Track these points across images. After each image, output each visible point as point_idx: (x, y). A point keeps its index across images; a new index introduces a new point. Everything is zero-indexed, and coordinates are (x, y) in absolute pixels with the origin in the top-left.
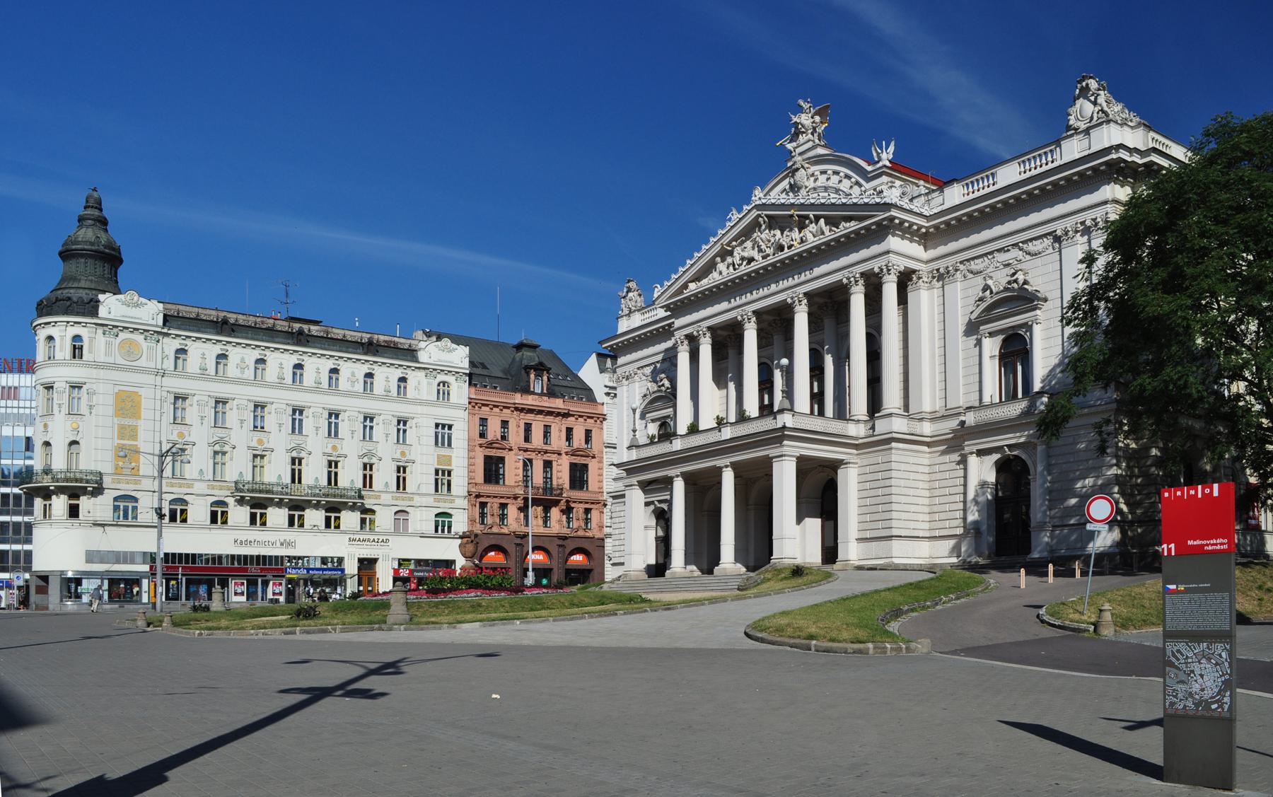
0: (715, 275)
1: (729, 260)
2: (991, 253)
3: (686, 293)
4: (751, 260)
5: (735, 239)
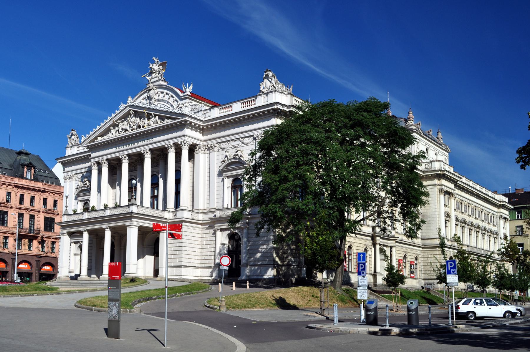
0: (110, 135)
1: (117, 129)
2: (229, 141)
3: (96, 142)
5: (119, 119)
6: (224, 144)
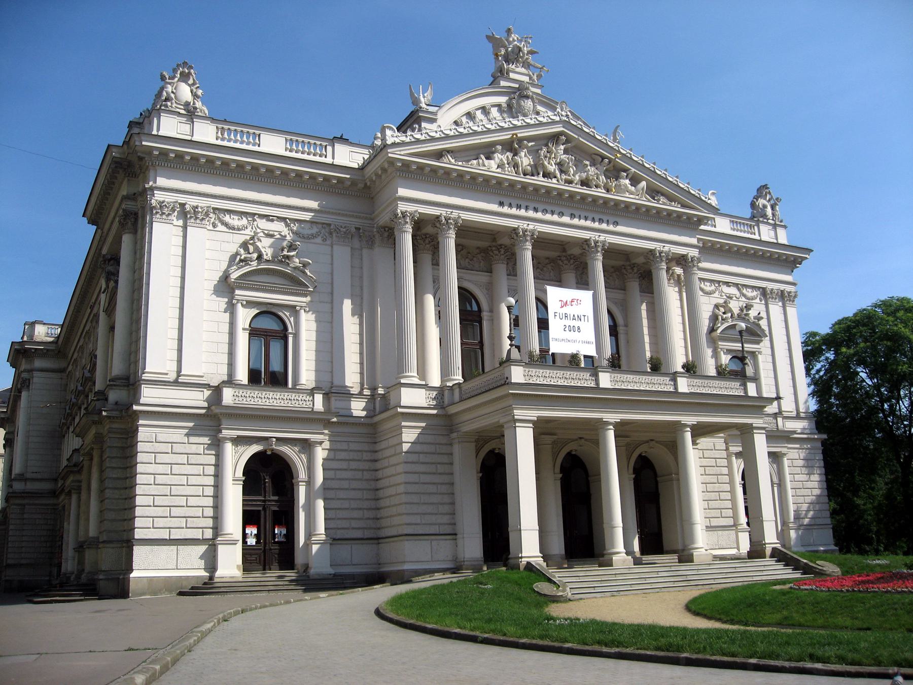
2: (719, 282)
4: (547, 175)
5: (529, 139)
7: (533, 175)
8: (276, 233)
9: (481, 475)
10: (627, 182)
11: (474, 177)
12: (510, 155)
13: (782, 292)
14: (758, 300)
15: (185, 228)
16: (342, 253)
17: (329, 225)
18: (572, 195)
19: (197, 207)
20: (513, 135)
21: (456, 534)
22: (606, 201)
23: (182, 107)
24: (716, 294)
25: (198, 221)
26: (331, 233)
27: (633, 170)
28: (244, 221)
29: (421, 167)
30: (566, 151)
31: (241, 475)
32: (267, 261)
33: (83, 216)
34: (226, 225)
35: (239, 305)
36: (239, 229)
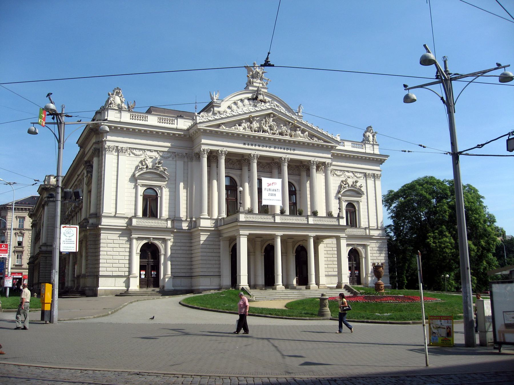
2: (344, 171)
5: (257, 117)
6: (339, 172)
7: (258, 132)
8: (153, 157)
9: (231, 253)
10: (300, 132)
11: (233, 134)
12: (249, 123)
13: (374, 174)
14: (362, 178)
15: (118, 156)
16: (180, 164)
17: (175, 153)
18: (275, 139)
19: (123, 148)
20: (250, 115)
21: (220, 276)
22: (290, 141)
23: (117, 106)
24: (343, 176)
25: (123, 153)
26: (175, 156)
27: (302, 127)
28: (141, 152)
29: (211, 131)
30: (273, 121)
31: (139, 252)
32: (150, 169)
33: (77, 143)
34: (134, 154)
35: (139, 186)
36: (139, 156)
